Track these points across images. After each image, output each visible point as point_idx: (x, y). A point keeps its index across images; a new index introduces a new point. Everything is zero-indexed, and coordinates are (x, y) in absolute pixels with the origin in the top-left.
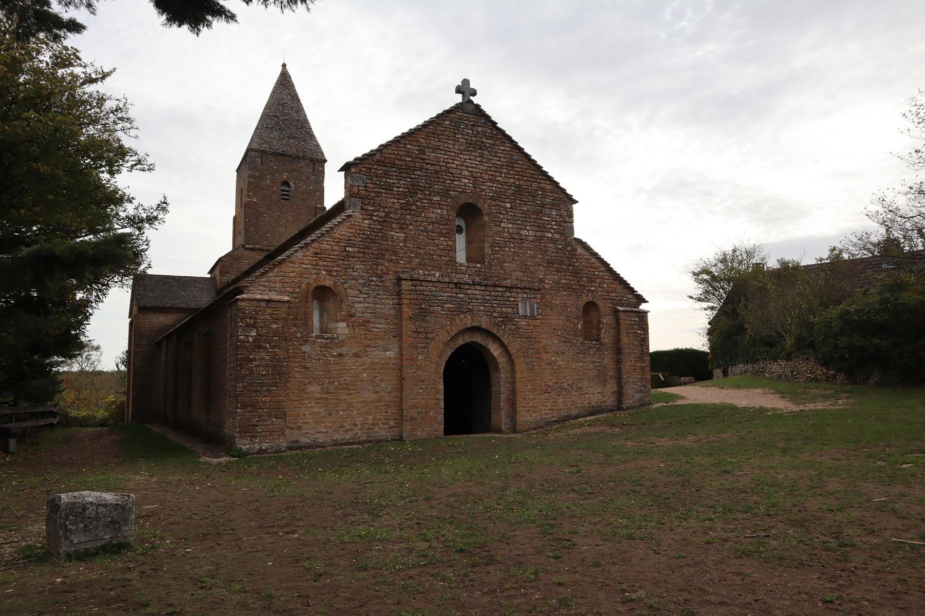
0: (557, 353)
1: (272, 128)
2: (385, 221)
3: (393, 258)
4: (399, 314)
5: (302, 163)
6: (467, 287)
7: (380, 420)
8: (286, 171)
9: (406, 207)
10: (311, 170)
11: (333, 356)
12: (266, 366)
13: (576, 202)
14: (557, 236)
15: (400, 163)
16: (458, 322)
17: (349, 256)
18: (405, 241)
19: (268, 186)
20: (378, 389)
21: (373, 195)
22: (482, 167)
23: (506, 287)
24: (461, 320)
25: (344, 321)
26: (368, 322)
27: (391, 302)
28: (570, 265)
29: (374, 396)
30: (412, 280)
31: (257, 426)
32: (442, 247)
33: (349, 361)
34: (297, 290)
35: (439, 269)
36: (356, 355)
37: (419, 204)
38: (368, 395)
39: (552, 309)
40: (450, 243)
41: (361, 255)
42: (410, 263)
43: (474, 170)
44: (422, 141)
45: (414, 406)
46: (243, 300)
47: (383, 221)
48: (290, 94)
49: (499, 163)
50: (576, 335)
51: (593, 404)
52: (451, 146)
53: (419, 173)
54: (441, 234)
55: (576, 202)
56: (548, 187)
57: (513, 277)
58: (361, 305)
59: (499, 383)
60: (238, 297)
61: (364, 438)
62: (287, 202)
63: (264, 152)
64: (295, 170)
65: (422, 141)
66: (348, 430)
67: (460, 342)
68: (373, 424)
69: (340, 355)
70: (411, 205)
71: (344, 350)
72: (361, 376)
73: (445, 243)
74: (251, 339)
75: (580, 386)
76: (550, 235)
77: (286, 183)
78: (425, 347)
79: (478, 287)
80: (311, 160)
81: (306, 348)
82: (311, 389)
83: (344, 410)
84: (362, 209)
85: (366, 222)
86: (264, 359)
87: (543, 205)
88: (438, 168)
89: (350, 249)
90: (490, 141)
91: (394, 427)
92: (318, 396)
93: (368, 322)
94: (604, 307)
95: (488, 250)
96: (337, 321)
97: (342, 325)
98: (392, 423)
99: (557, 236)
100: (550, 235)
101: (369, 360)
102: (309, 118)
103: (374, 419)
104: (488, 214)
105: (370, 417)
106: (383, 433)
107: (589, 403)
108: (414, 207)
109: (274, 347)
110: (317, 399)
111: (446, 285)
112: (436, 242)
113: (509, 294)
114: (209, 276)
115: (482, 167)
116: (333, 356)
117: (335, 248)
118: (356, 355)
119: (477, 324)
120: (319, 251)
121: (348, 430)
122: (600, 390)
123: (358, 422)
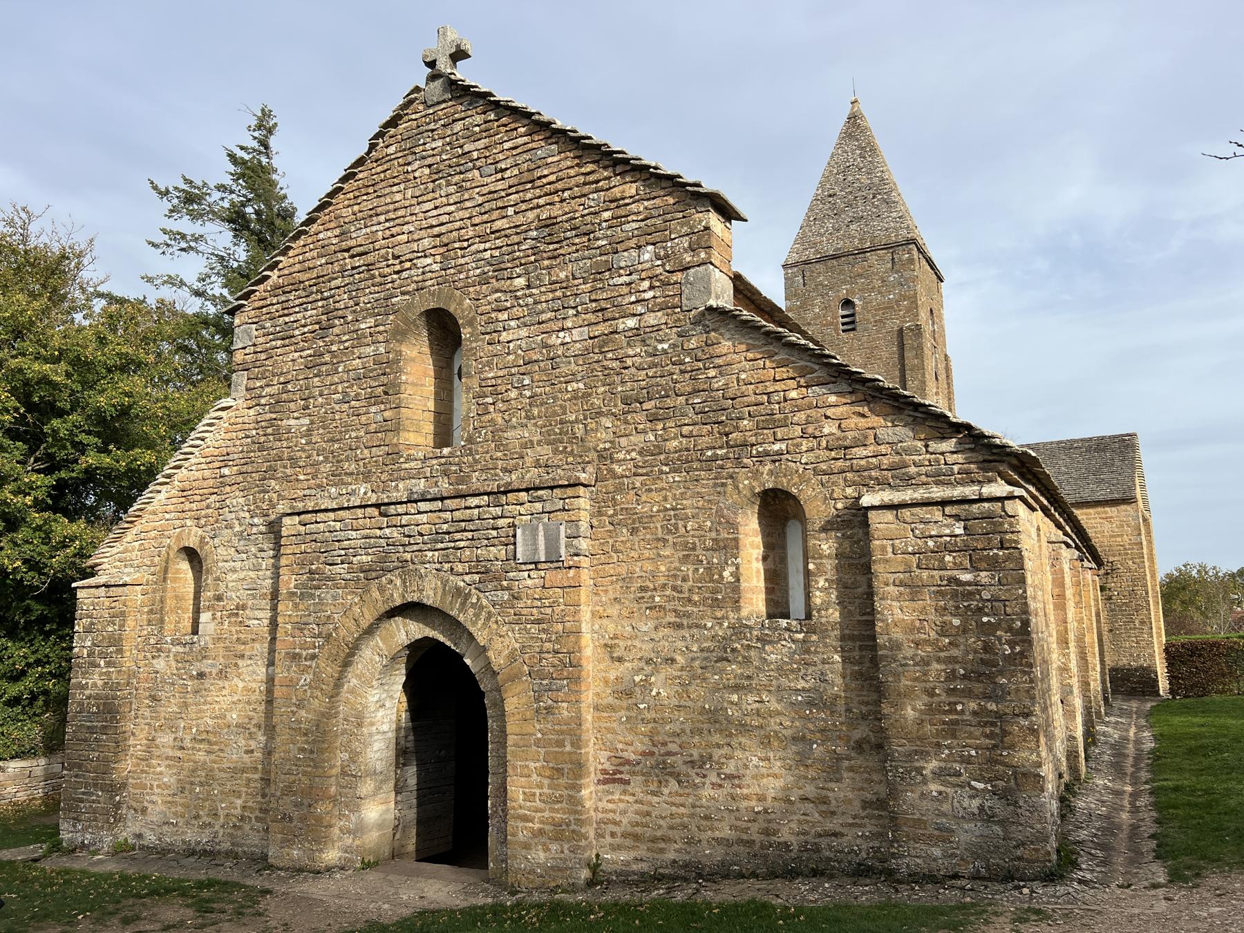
0: (649, 661)
3: (289, 471)
5: (872, 258)
6: (401, 509)
8: (844, 282)
10: (890, 265)
11: (191, 677)
12: (97, 697)
14: (651, 319)
15: (308, 276)
16: (376, 594)
17: (222, 482)
18: (309, 432)
19: (817, 316)
20: (253, 745)
21: (263, 356)
22: (461, 214)
23: (488, 494)
24: (381, 589)
26: (244, 607)
28: (696, 391)
30: (299, 514)
31: (82, 801)
32: (373, 427)
34: (157, 559)
35: (367, 476)
37: (334, 348)
39: (634, 531)
40: (387, 414)
41: (240, 478)
42: (315, 477)
43: (443, 229)
44: (344, 212)
45: (288, 790)
46: (83, 588)
47: (277, 404)
49: (500, 185)
50: (717, 604)
51: (785, 835)
52: (398, 197)
54: (373, 399)
56: (631, 189)
57: (529, 461)
58: (235, 576)
60: (74, 585)
61: (227, 846)
62: (852, 334)
63: (806, 263)
64: (860, 275)
65: (344, 212)
66: (205, 826)
68: (242, 818)
69: (201, 675)
70: (322, 355)
71: (205, 666)
72: (228, 717)
73: (379, 418)
74: (85, 651)
75: (730, 768)
76: (631, 323)
77: (848, 303)
78: (313, 657)
79: (423, 506)
80: (887, 247)
83: (201, 784)
84: (247, 390)
85: (252, 412)
86: (95, 685)
88: (370, 258)
89: (226, 471)
90: (481, 144)
92: (171, 754)
93: (244, 607)
94: (819, 504)
99: (651, 319)
100: (631, 323)
101: (241, 685)
104: (471, 323)
105: (239, 802)
107: (767, 832)
108: (327, 358)
109: (108, 664)
111: (360, 512)
112: (363, 418)
113: (498, 511)
115: (461, 214)
116: (191, 677)
117: (207, 473)
119: (414, 597)
120: (187, 485)
121: (205, 826)
122: (810, 790)
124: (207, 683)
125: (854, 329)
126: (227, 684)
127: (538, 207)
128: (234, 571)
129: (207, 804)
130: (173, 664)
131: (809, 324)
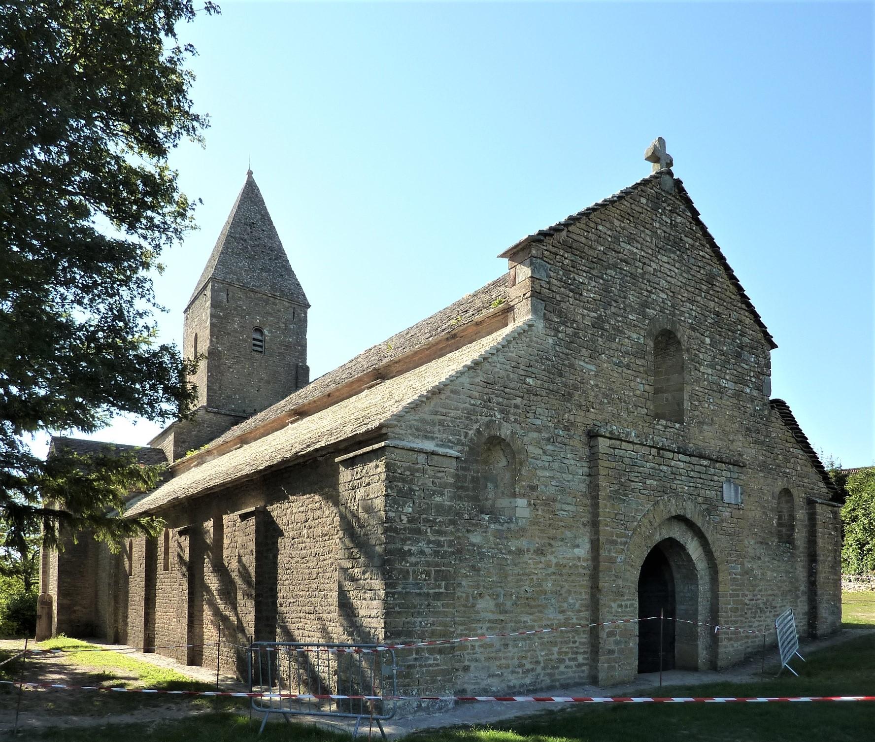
1: (239, 254)
2: (572, 342)
4: (594, 490)
7: (566, 653)
9: (598, 324)
11: (510, 552)
13: (774, 346)
22: (681, 279)
25: (524, 496)
27: (580, 472)
29: (561, 617)
33: (529, 559)
36: (540, 552)
38: (552, 615)
48: (259, 212)
53: (613, 273)
55: (774, 346)
56: (747, 321)
59: (694, 599)
61: (547, 681)
67: (658, 538)
81: (476, 538)
82: (481, 604)
87: (741, 347)
91: (583, 665)
92: (491, 616)
95: (687, 405)
96: (514, 495)
97: (521, 502)
98: (580, 659)
101: (554, 561)
102: (285, 246)
103: (559, 653)
105: (555, 649)
106: (571, 674)
110: (489, 621)
114: (149, 446)
116: (510, 552)
118: (540, 552)
121: (528, 671)
123: (541, 659)
124: (526, 557)
125: (261, 352)
126: (543, 559)
127: (714, 301)
128: (544, 469)
129: (529, 654)
130: (491, 538)
131: (229, 334)
